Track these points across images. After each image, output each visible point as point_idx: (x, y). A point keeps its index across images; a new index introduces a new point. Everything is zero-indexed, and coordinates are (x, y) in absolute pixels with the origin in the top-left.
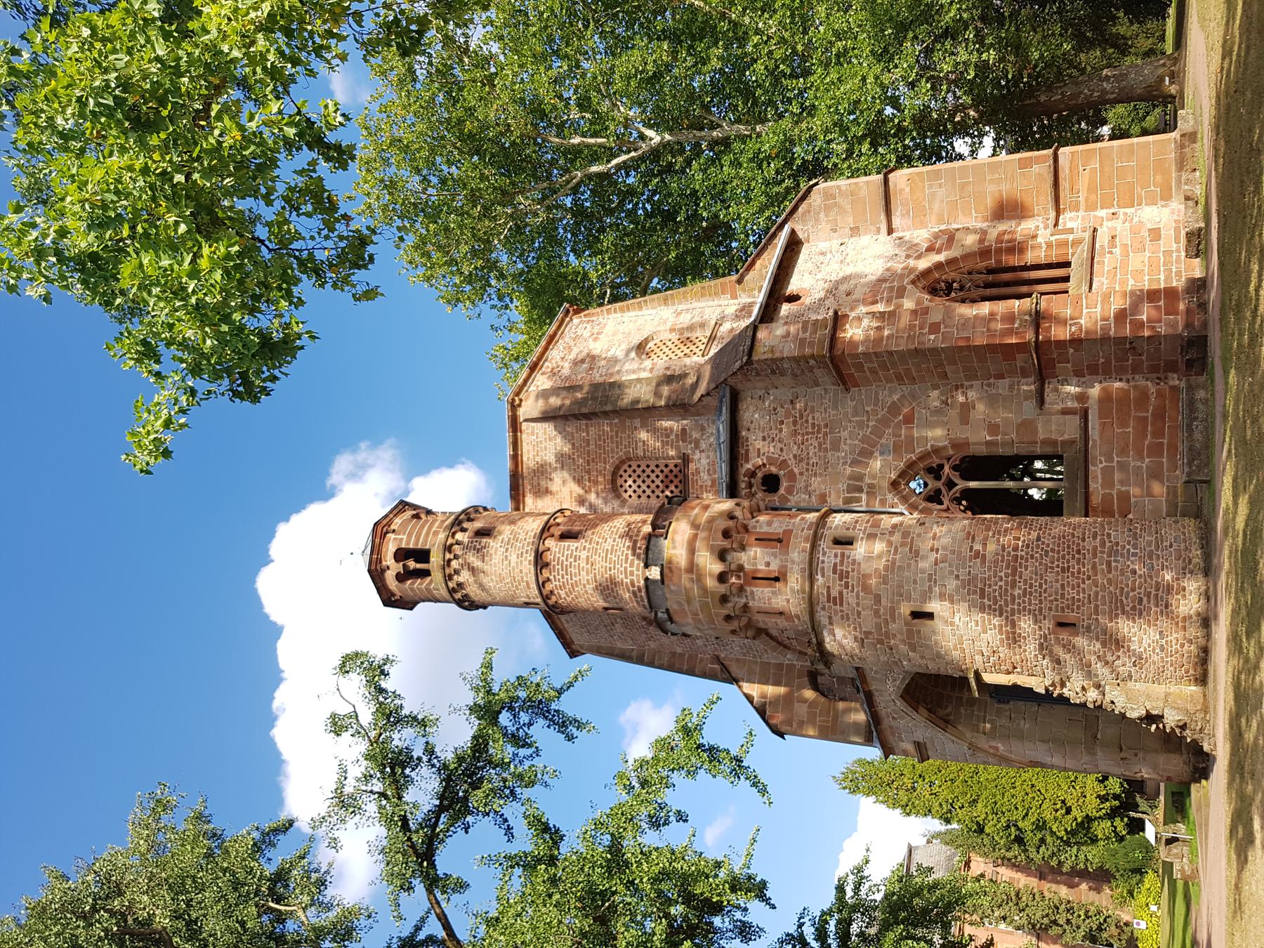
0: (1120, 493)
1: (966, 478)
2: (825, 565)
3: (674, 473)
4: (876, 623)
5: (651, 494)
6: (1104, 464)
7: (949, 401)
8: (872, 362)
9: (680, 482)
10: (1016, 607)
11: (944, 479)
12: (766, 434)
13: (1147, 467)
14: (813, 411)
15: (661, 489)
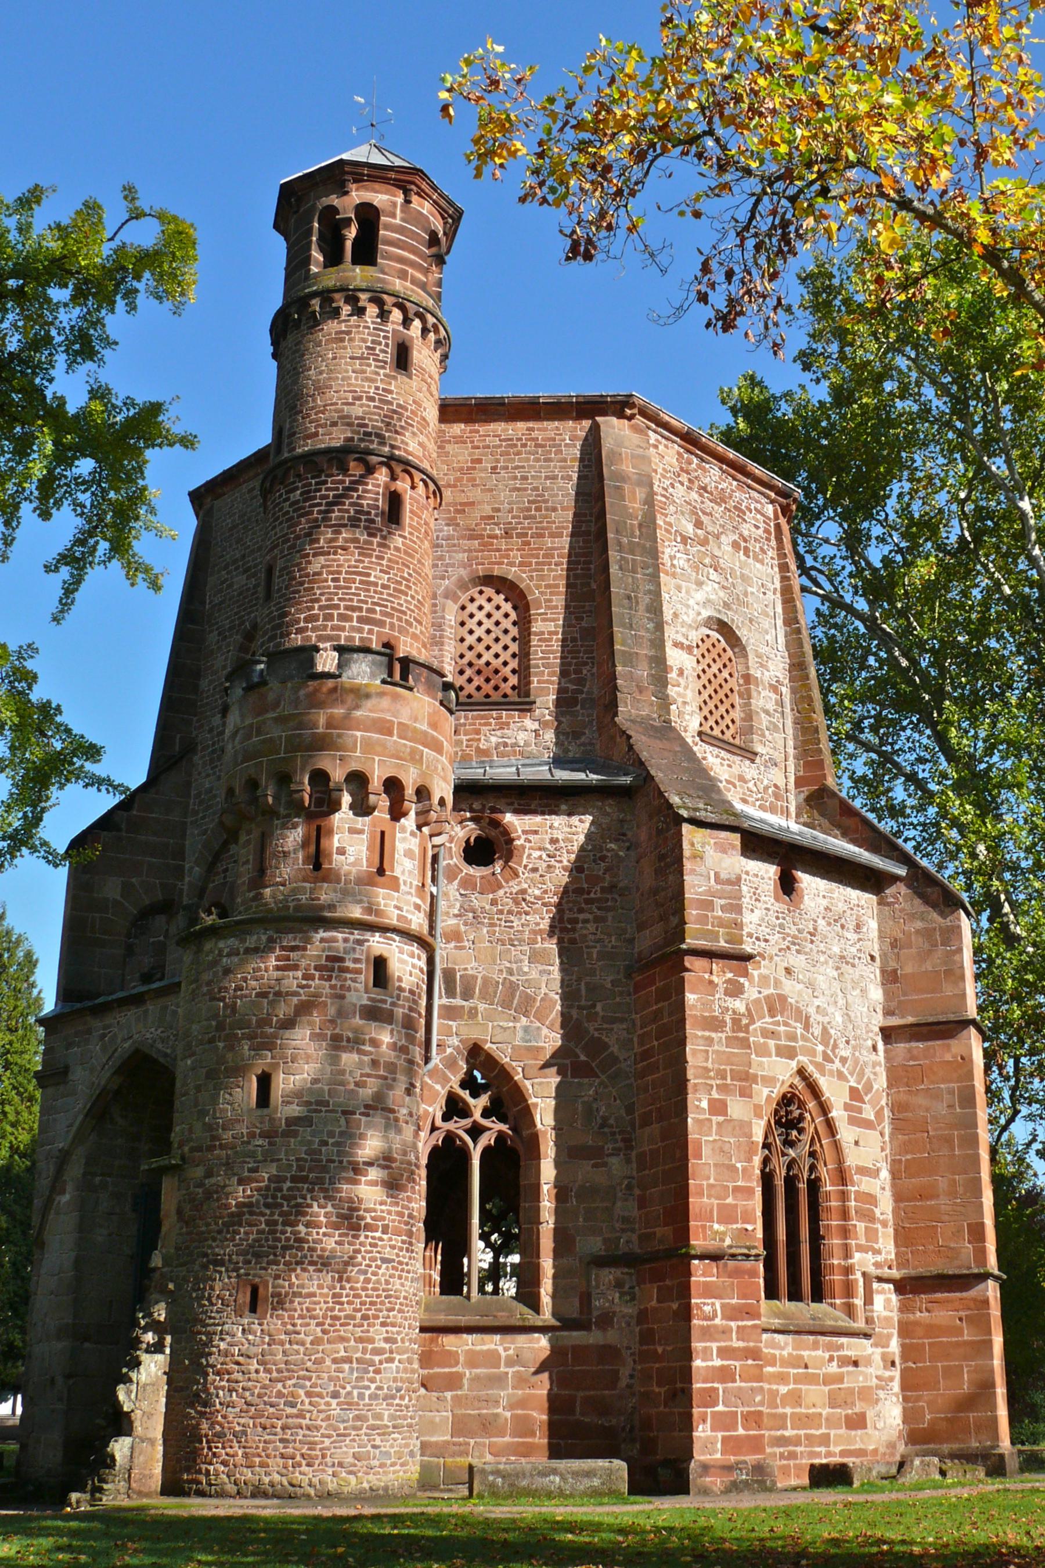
0: (460, 1376)
6: (503, 1354)
7: (606, 1130)
8: (670, 1014)
9: (487, 696)
10: (280, 1228)
12: (562, 844)
13: (497, 1415)
14: (597, 920)
15: (475, 661)
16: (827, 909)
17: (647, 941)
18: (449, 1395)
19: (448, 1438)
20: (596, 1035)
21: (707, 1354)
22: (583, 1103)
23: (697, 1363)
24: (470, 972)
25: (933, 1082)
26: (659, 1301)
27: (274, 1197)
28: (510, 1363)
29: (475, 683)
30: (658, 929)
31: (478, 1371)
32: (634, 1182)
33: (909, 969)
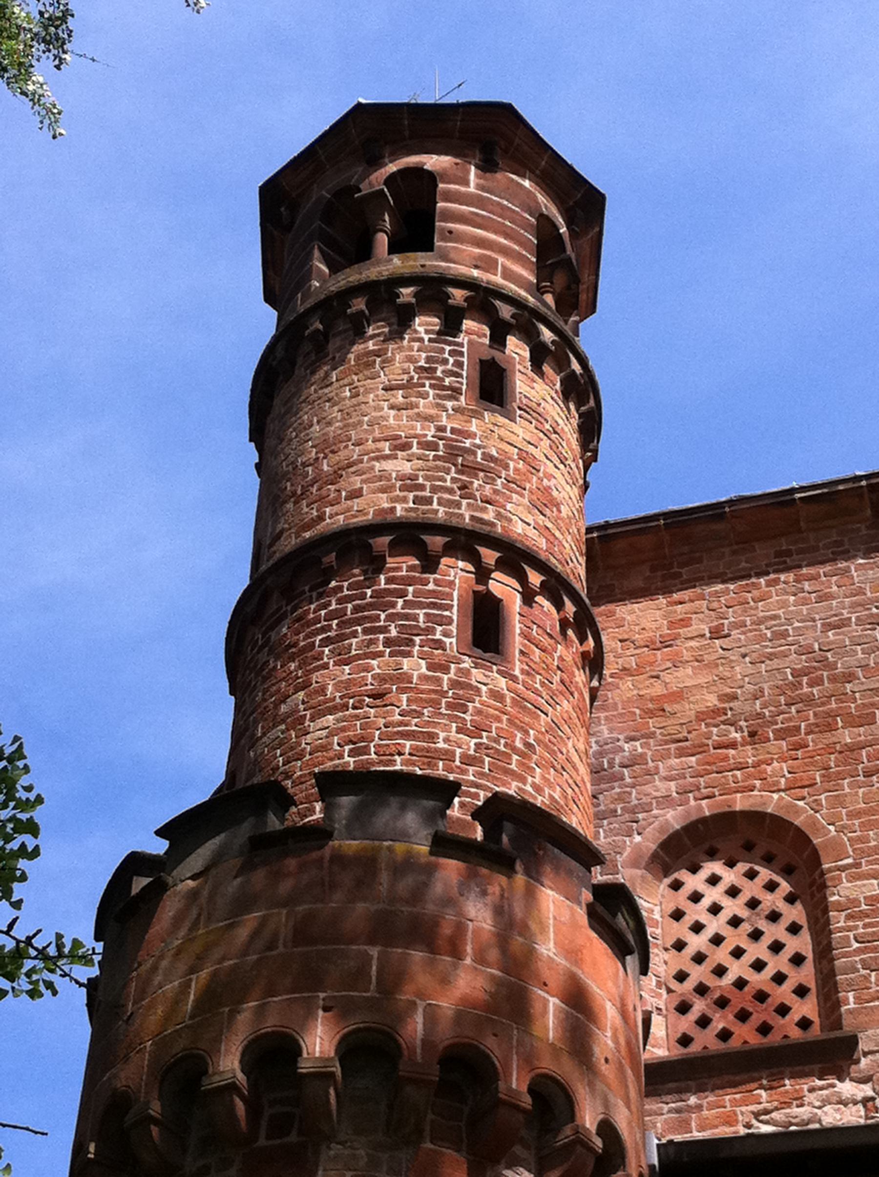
3: (778, 1021)
5: (690, 951)
15: (711, 981)
29: (718, 1024)
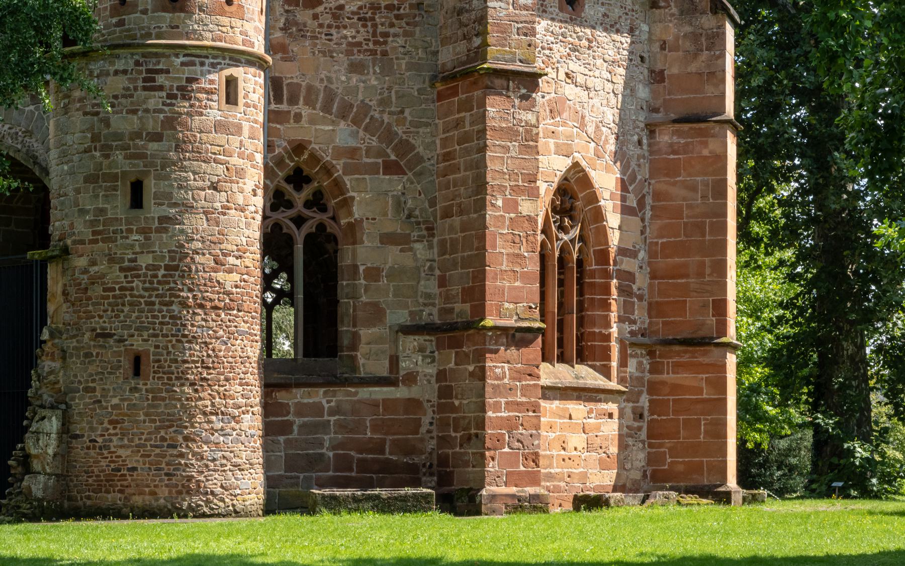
0: (290, 424)
1: (309, 240)
2: (198, 68)
4: (122, 134)
6: (326, 406)
7: (413, 220)
8: (472, 124)
10: (157, 307)
11: (307, 213)
13: (322, 455)
14: (406, 34)
16: (605, 15)
17: (447, 56)
18: (282, 439)
19: (282, 473)
20: (404, 137)
21: (497, 407)
22: (393, 196)
23: (490, 414)
24: (295, 81)
25: (690, 175)
26: (456, 364)
27: (151, 283)
28: (332, 412)
30: (462, 47)
31: (306, 419)
32: (435, 265)
33: (675, 70)
